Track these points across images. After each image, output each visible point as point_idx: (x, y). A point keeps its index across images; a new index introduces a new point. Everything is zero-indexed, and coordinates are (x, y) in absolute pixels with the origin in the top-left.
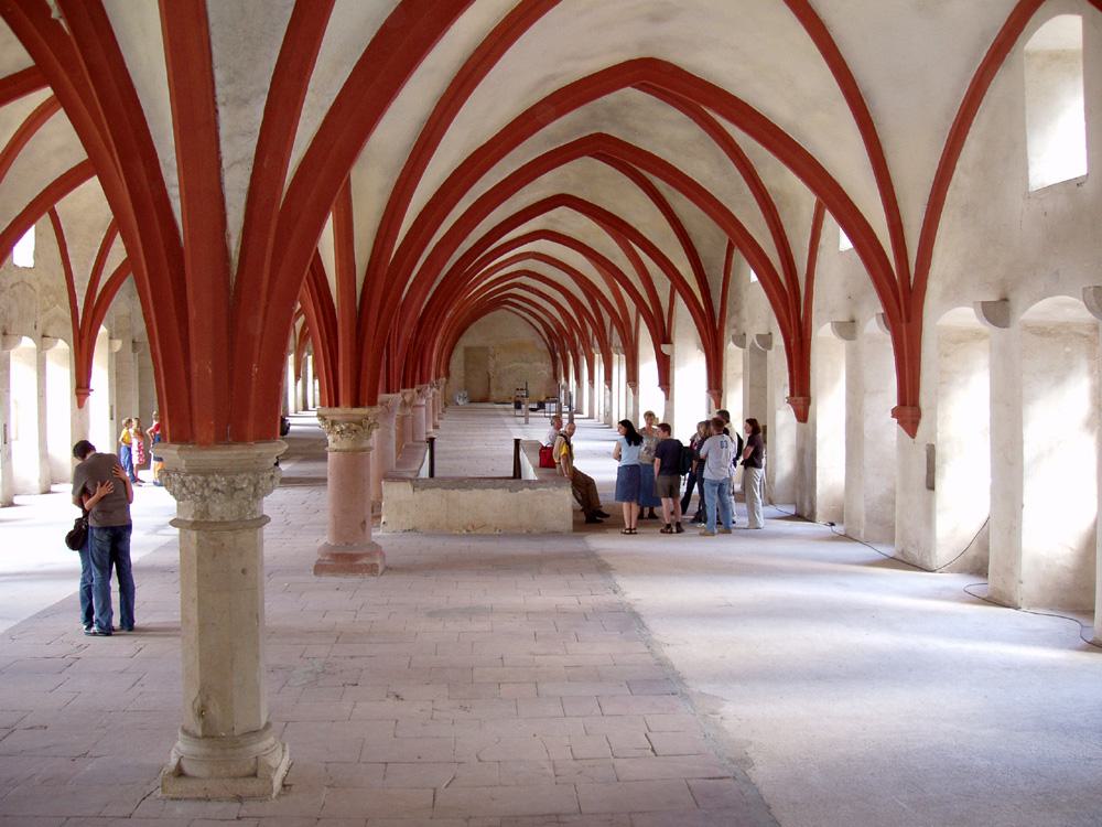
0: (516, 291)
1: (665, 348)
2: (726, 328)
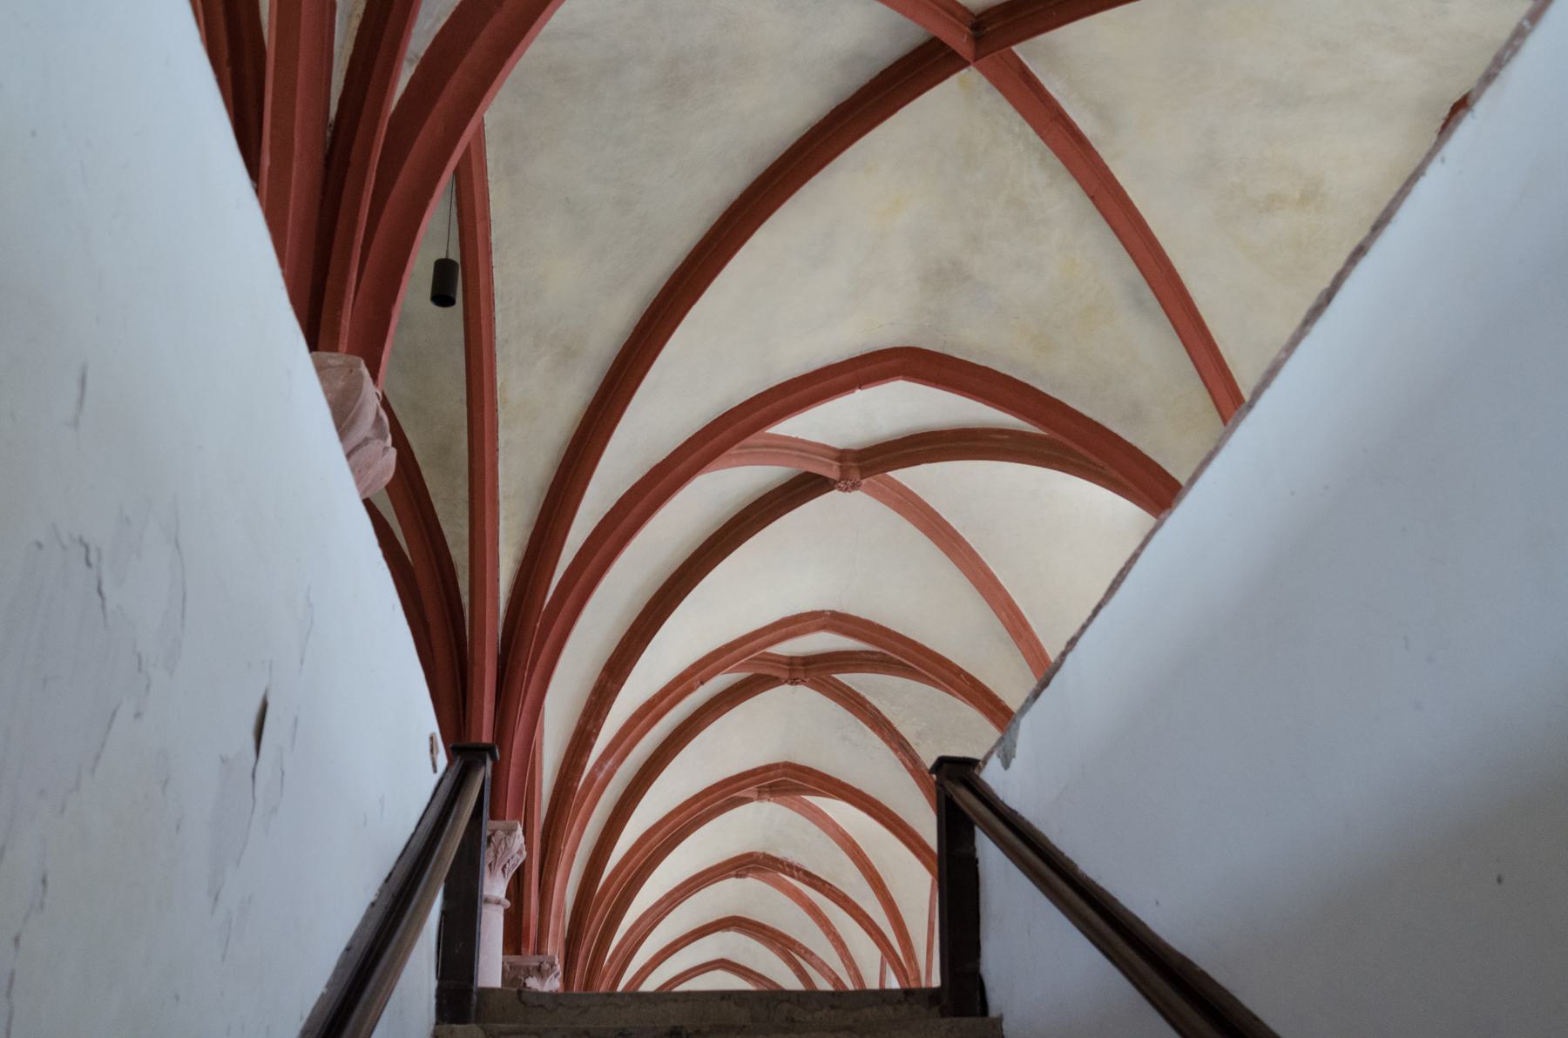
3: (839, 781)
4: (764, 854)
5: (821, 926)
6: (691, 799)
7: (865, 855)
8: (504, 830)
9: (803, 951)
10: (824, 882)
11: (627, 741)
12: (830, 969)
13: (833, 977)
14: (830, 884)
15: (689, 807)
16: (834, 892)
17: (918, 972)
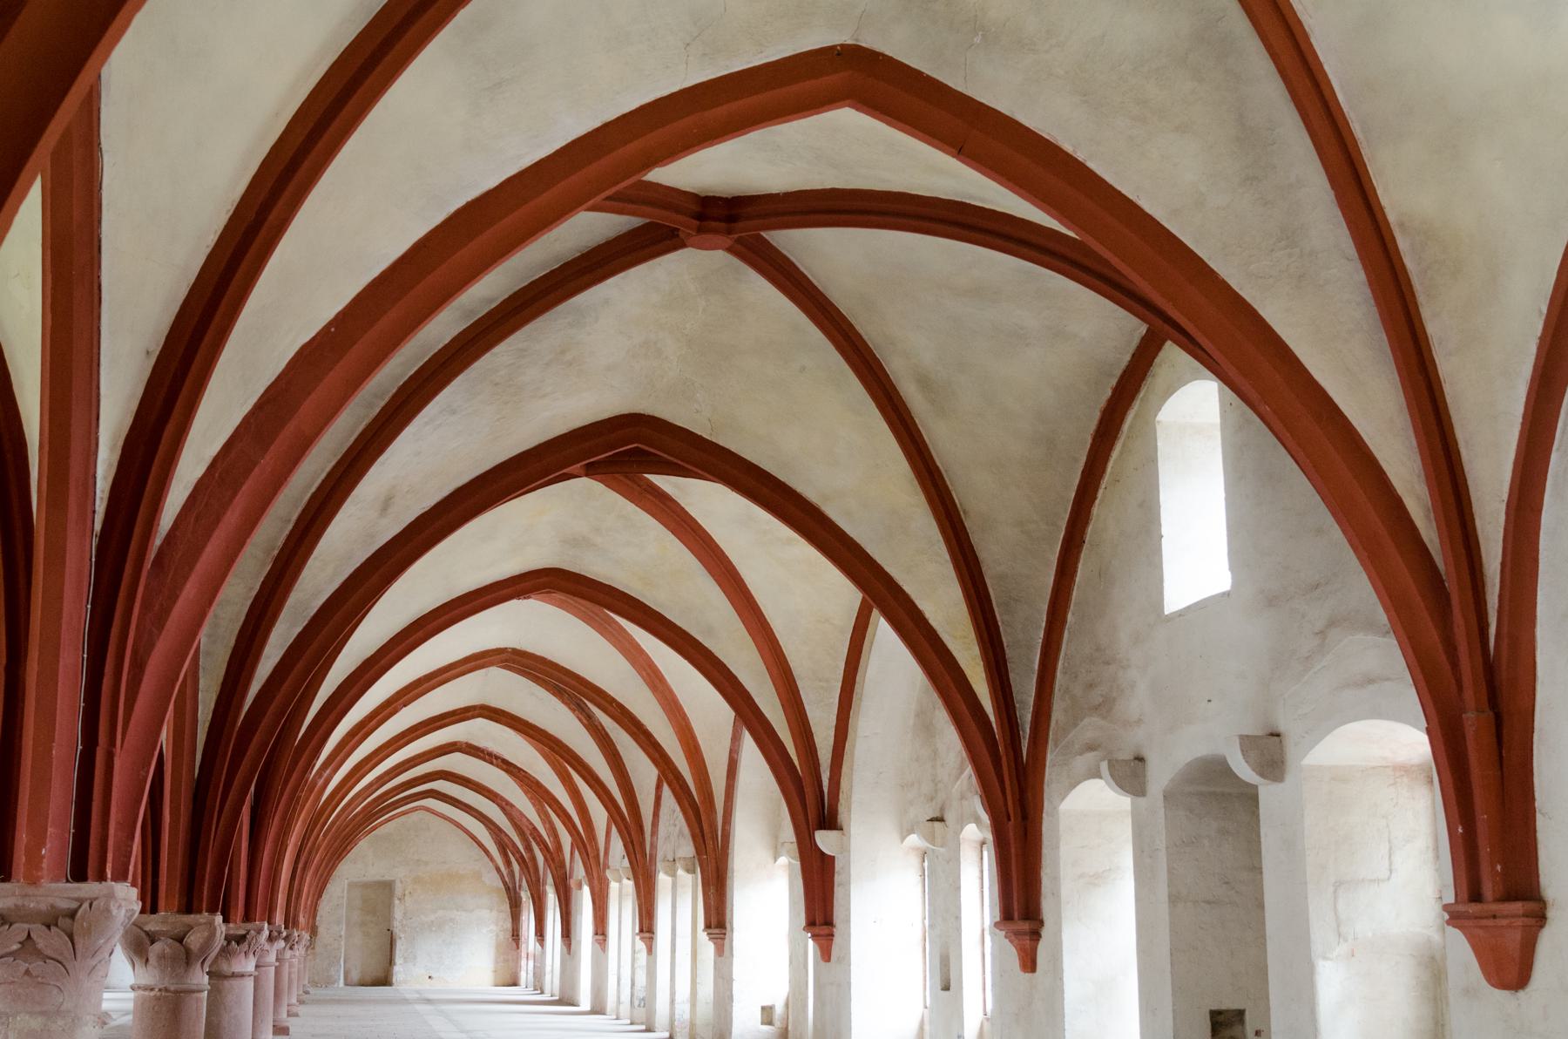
0: (456, 762)
1: (825, 840)
2: (1050, 757)
4: (466, 743)
8: (254, 930)
9: (504, 803)
11: (342, 754)
12: (528, 820)
13: (531, 827)
14: (524, 771)
16: (526, 777)
17: (598, 850)
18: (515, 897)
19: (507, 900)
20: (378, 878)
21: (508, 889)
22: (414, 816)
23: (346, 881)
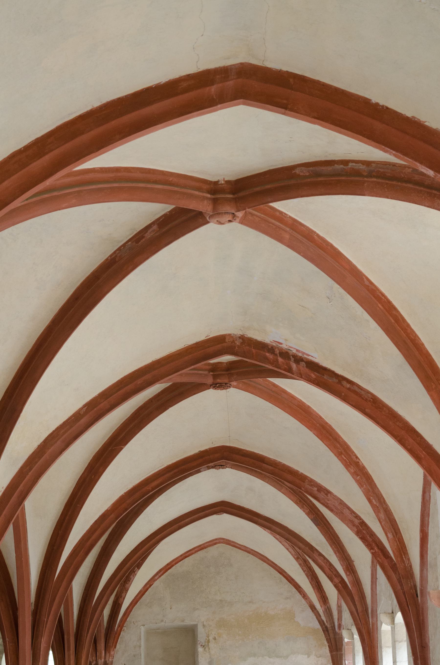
3: (366, 102)
4: (242, 337)
5: (339, 455)
6: (27, 148)
7: (408, 325)
10: (341, 379)
12: (352, 512)
13: (357, 521)
15: (24, 165)
18: (335, 639)
19: (326, 643)
20: (178, 623)
21: (325, 630)
22: (213, 551)
23: (143, 628)
